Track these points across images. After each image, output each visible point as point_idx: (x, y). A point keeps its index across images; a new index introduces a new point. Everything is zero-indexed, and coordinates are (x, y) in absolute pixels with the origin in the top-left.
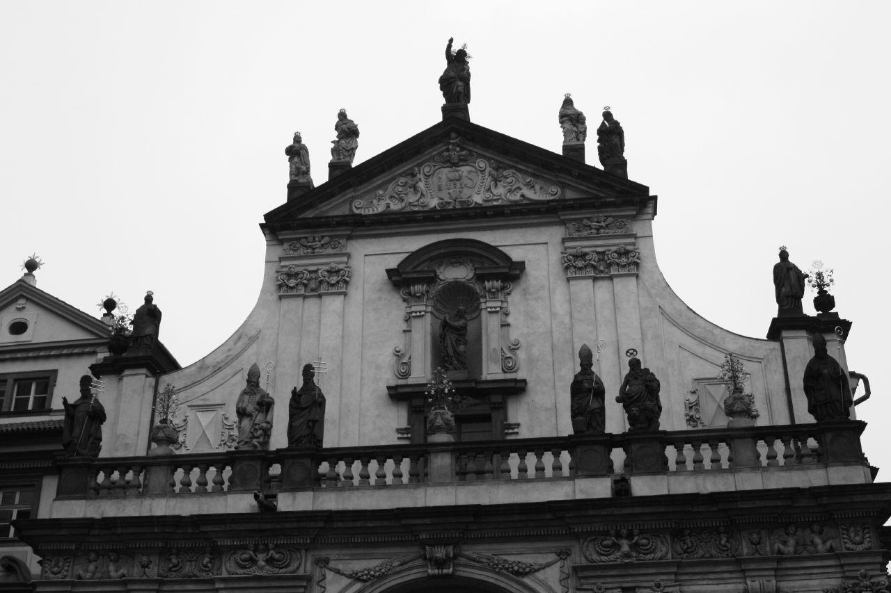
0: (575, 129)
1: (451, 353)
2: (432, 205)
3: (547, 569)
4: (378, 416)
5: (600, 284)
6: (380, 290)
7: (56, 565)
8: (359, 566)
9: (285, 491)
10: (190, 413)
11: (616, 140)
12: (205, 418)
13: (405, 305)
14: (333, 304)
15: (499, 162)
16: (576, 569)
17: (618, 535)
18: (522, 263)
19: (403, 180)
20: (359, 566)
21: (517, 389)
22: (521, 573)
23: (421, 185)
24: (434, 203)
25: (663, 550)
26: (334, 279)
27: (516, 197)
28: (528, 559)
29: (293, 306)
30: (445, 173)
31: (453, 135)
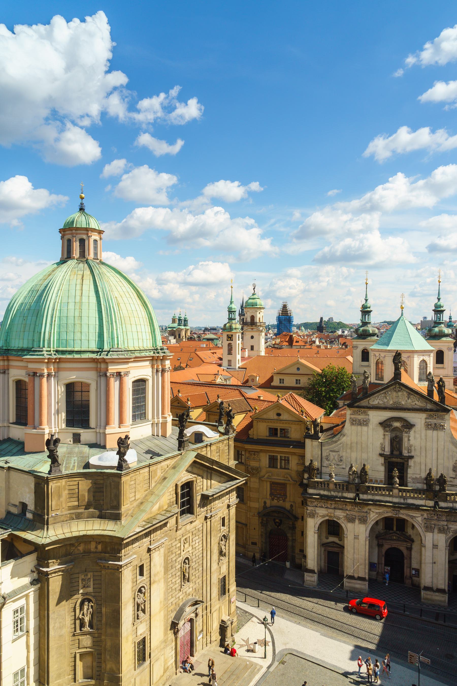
0: (431, 384)
1: (395, 447)
2: (391, 404)
3: (419, 518)
4: (377, 459)
5: (434, 431)
6: (377, 426)
7: (311, 503)
8: (378, 511)
9: (361, 494)
10: (331, 453)
11: (443, 389)
12: (334, 454)
13: (383, 431)
14: (365, 428)
15: (409, 393)
16: (425, 519)
17: (434, 514)
18: (415, 425)
19: (383, 395)
20: (378, 511)
21: (412, 457)
22: (413, 517)
23: (388, 398)
24: (391, 402)
25: (444, 518)
26: (365, 423)
27: (414, 404)
28: (414, 515)
29: (354, 428)
30: (394, 394)
31: (397, 384)
